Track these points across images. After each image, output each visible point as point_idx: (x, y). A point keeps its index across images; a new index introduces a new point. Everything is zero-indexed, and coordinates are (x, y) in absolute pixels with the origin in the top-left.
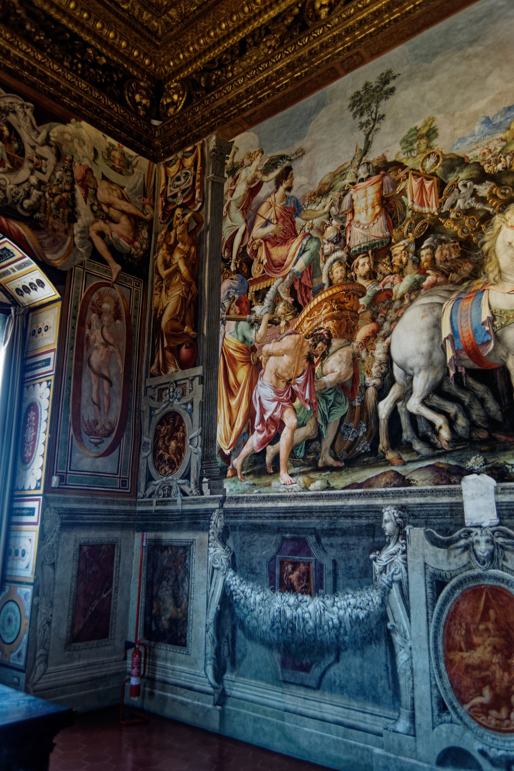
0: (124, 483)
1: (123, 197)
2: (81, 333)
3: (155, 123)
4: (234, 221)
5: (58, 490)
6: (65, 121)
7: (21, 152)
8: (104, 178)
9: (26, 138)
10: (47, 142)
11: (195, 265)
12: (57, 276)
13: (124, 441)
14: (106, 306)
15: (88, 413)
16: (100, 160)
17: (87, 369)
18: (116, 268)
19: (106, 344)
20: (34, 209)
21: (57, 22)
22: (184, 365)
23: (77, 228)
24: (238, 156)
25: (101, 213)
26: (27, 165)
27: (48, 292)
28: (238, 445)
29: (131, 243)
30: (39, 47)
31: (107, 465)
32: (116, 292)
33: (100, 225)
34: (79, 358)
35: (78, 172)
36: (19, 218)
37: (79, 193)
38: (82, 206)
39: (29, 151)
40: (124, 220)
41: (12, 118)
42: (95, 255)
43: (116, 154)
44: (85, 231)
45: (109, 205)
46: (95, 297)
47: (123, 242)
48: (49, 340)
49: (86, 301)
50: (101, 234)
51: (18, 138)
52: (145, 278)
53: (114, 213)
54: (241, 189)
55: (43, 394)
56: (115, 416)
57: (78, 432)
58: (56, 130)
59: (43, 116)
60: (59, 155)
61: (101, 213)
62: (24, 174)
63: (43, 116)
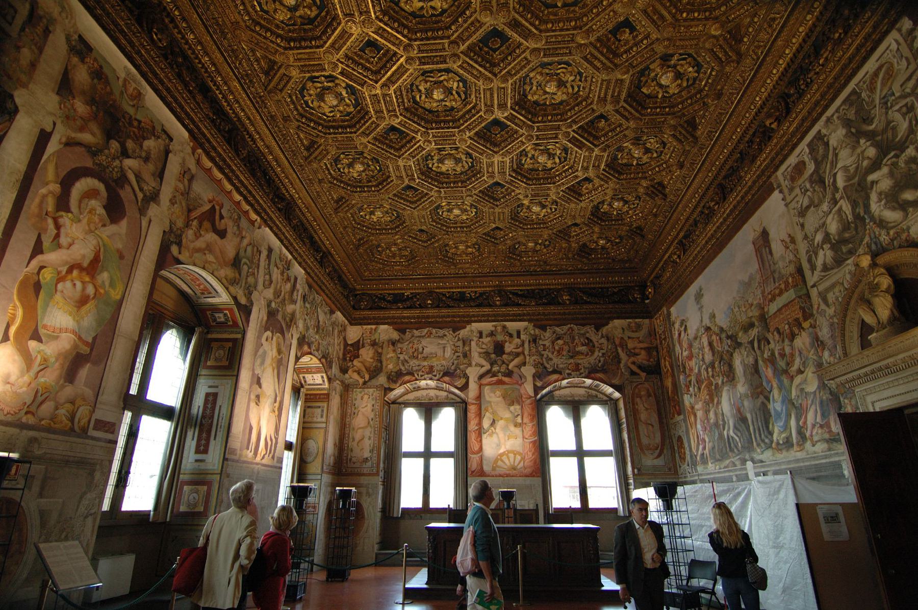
0: (670, 469)
1: (640, 342)
2: (634, 408)
3: (647, 301)
4: (677, 348)
5: (639, 474)
6: (607, 324)
7: (594, 346)
8: (629, 338)
9: (594, 339)
10: (602, 337)
11: (672, 367)
12: (617, 388)
13: (665, 451)
14: (642, 393)
15: (645, 441)
16: (626, 332)
17: (640, 423)
18: (643, 375)
19: (647, 409)
20: (603, 366)
21: (594, 288)
22: (679, 414)
23: (622, 365)
24: (673, 318)
25: (632, 354)
26: (597, 350)
27: (617, 395)
28: (697, 450)
29: (648, 361)
30: (589, 303)
31: (660, 462)
32: (646, 385)
33: (632, 359)
34: (635, 419)
35: (617, 342)
36: (597, 372)
37: (620, 350)
38: (623, 355)
39: (596, 344)
40: (643, 352)
41: (588, 335)
42: (633, 373)
43: (633, 325)
44: (626, 365)
45: (634, 349)
46: (637, 391)
47: (644, 362)
48: (623, 413)
49: (633, 394)
50: (634, 363)
51: (591, 341)
52: (660, 374)
53: (637, 351)
54: (677, 333)
55: (625, 436)
56: (658, 439)
57: (641, 449)
58: (605, 330)
59: (598, 328)
60: (608, 339)
61: (632, 354)
62: (596, 353)
63: (598, 328)
